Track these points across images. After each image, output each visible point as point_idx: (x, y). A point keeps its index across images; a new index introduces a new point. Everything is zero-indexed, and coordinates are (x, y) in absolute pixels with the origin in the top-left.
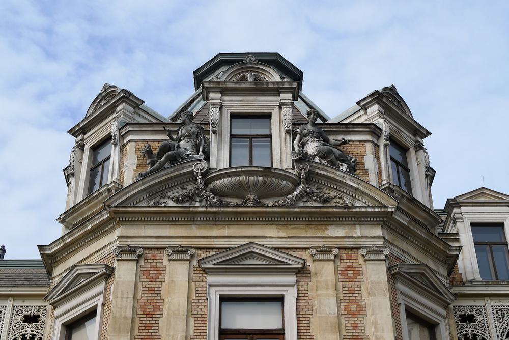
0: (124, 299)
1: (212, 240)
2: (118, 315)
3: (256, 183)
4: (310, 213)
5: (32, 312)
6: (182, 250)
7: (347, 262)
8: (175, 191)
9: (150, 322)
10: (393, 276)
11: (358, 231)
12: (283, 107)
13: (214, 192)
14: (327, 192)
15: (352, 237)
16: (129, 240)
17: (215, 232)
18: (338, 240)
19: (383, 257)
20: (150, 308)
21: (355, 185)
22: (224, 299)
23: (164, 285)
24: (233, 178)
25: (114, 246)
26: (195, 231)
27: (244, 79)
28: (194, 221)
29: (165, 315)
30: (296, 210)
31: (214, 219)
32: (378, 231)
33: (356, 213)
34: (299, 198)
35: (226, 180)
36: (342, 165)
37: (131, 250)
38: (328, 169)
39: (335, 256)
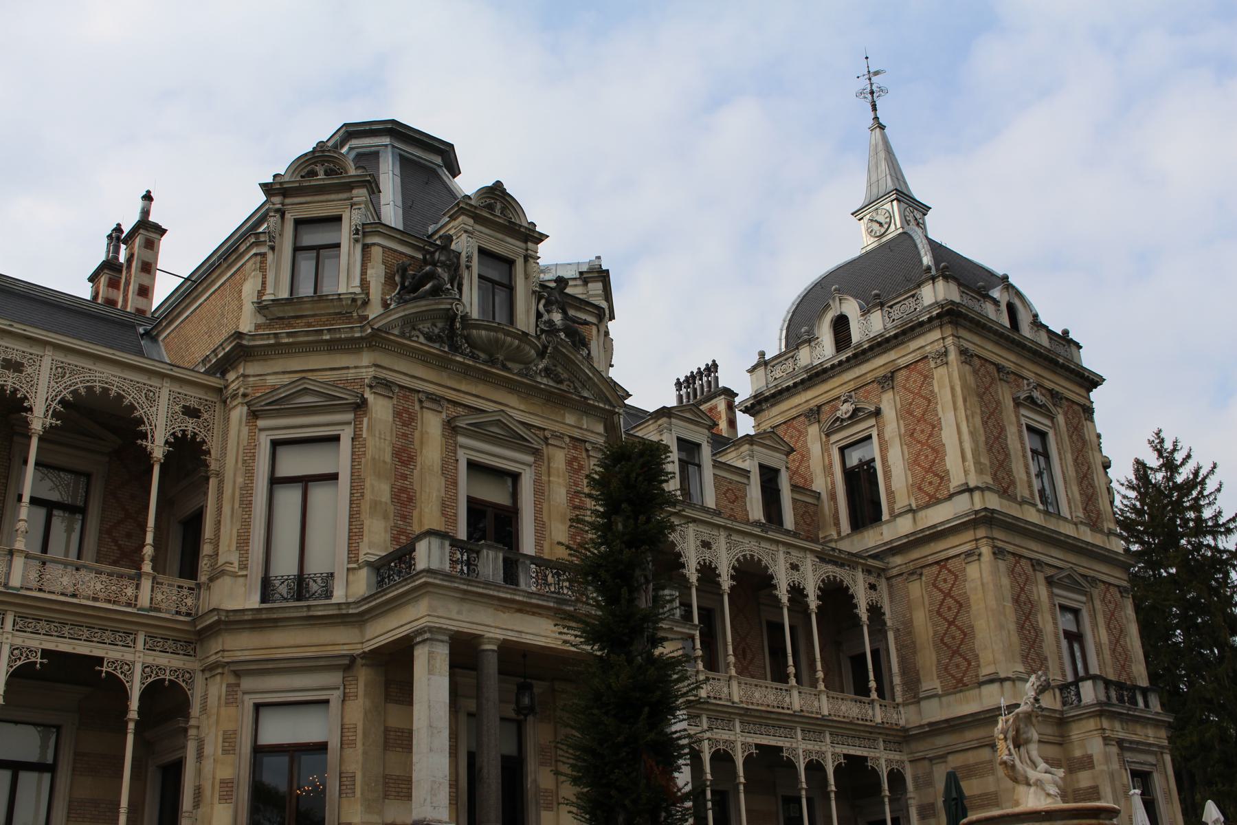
0: (382, 441)
1: (462, 395)
2: (377, 457)
3: (511, 345)
4: (551, 393)
5: (193, 403)
6: (435, 399)
8: (426, 325)
9: (406, 472)
12: (531, 261)
13: (467, 338)
14: (561, 371)
15: (581, 429)
16: (385, 372)
17: (463, 387)
18: (569, 428)
21: (591, 375)
23: (417, 434)
24: (492, 334)
27: (490, 207)
28: (447, 368)
29: (418, 468)
30: (542, 386)
31: (466, 372)
33: (589, 404)
35: (483, 333)
36: (583, 350)
38: (570, 349)
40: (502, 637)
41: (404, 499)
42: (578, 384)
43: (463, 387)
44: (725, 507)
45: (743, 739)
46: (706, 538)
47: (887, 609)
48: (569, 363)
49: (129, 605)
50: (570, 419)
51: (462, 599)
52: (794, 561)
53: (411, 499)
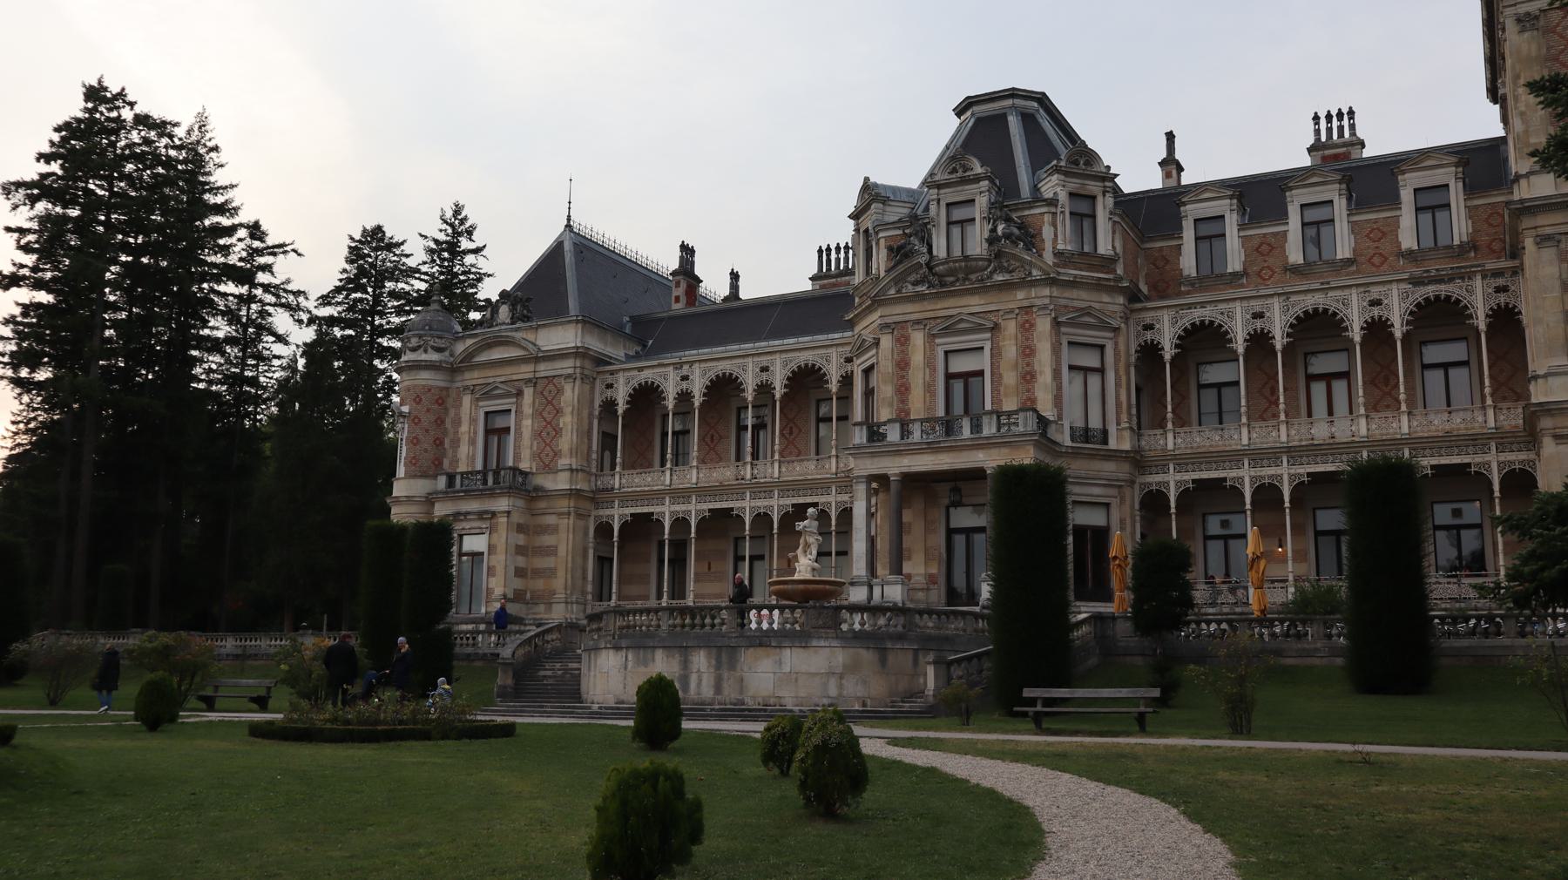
3: (960, 267)
6: (918, 322)
7: (1026, 317)
10: (1056, 324)
11: (1033, 293)
19: (1049, 312)
20: (903, 364)
22: (946, 353)
25: (876, 324)
26: (927, 305)
31: (938, 296)
32: (1047, 292)
34: (992, 273)
35: (941, 267)
37: (887, 326)
39: (1017, 315)
40: (897, 472)
41: (903, 390)
42: (1027, 267)
43: (939, 307)
44: (1369, 247)
45: (1292, 471)
46: (1258, 309)
47: (1523, 308)
48: (1014, 256)
49: (827, 473)
50: (1020, 295)
51: (872, 457)
52: (1375, 296)
53: (907, 389)
